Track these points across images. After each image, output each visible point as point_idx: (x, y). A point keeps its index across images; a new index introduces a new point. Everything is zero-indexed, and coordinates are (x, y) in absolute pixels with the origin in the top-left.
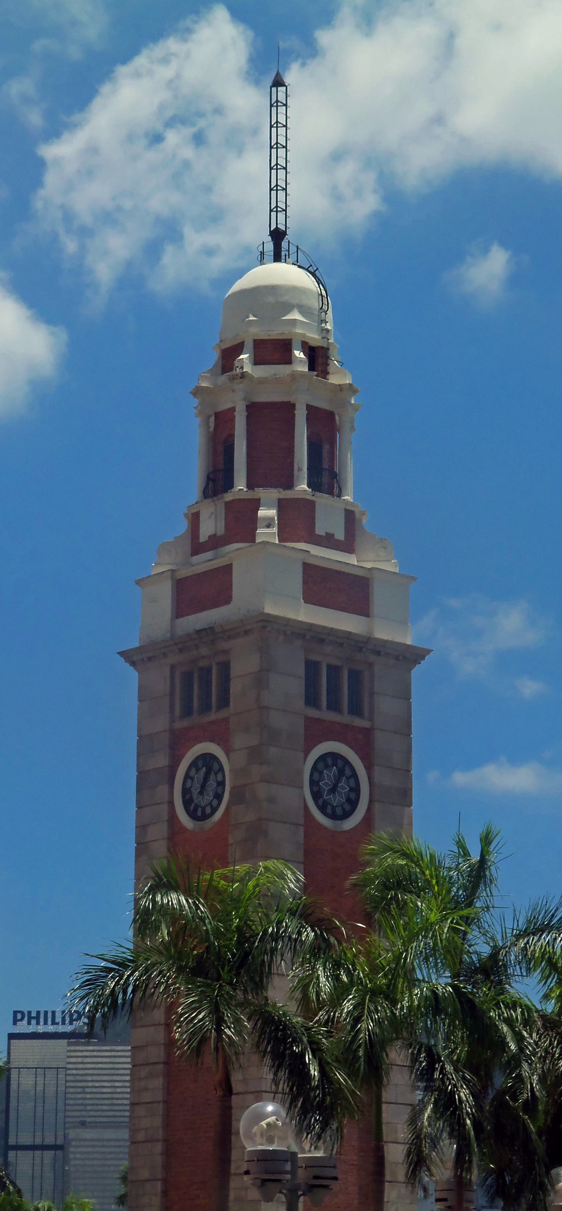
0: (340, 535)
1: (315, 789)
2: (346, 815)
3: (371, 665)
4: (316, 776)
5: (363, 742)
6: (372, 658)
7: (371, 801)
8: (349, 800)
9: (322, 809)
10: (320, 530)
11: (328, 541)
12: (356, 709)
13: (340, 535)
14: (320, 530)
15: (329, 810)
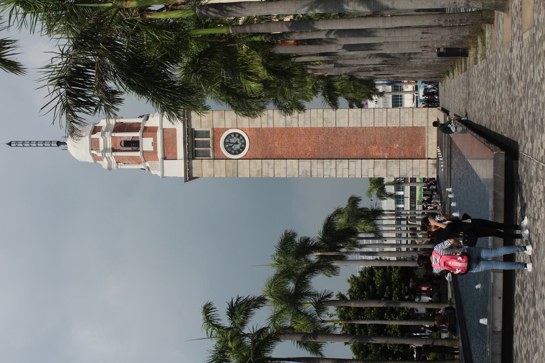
0: (151, 140)
1: (237, 152)
2: (244, 138)
3: (192, 129)
4: (233, 152)
5: (217, 132)
6: (190, 130)
7: (237, 128)
8: (239, 137)
9: (243, 149)
10: (151, 149)
11: (154, 144)
12: (208, 132)
13: (151, 140)
14: (151, 149)
15: (243, 146)
